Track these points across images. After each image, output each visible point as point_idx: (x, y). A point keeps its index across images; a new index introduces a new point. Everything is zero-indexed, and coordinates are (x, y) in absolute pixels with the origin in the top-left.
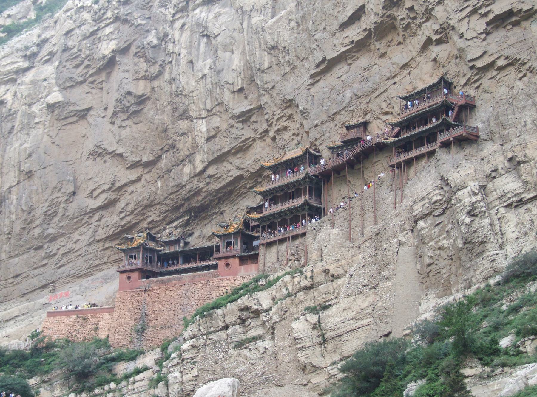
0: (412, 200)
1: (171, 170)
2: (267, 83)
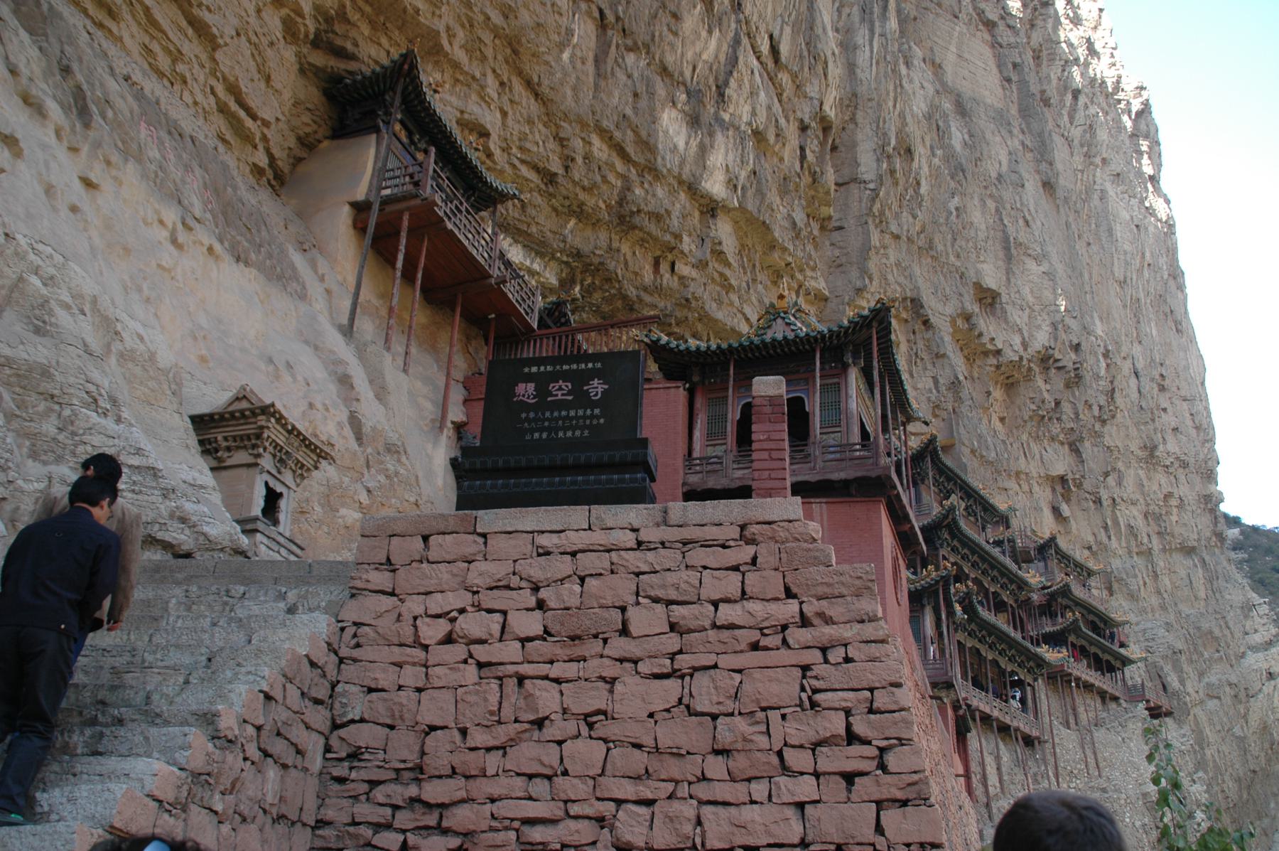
2: (890, 208)
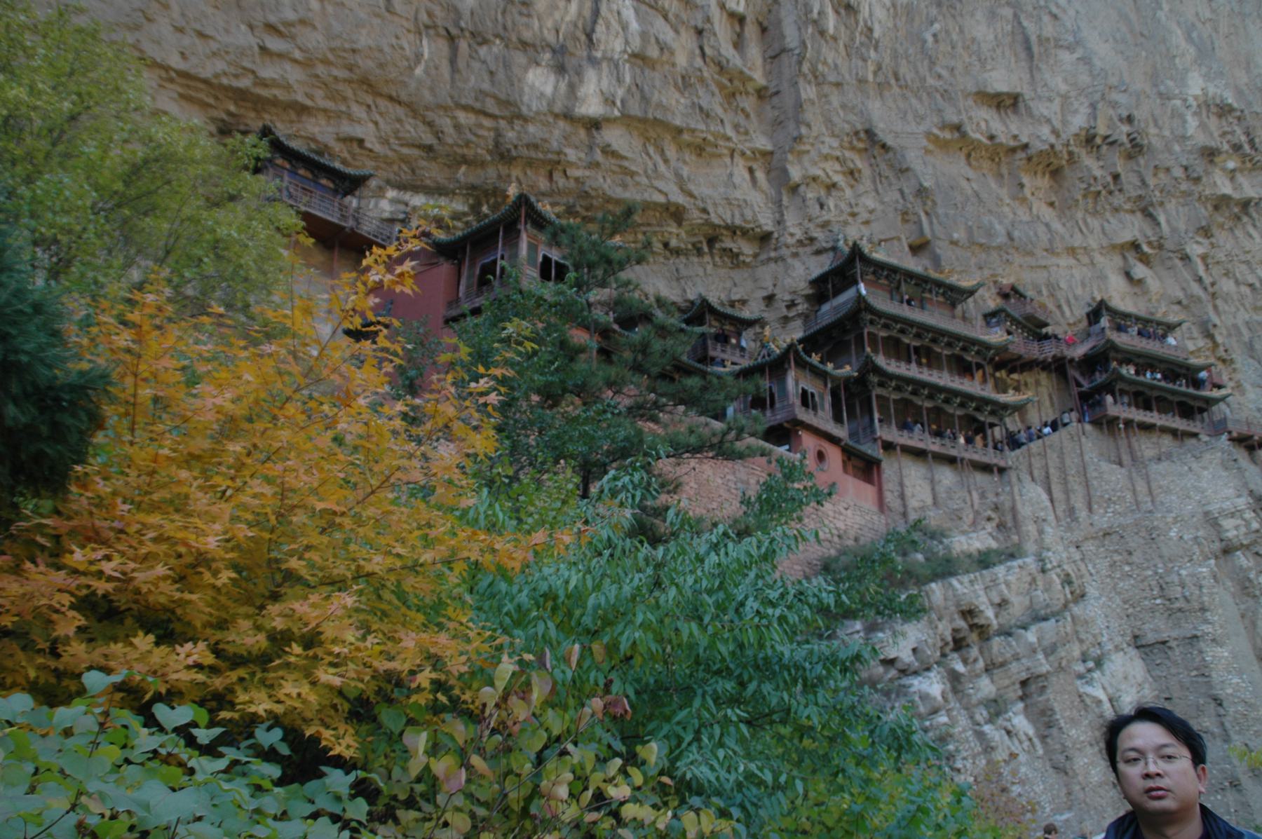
1: (485, 42)
2: (825, 63)
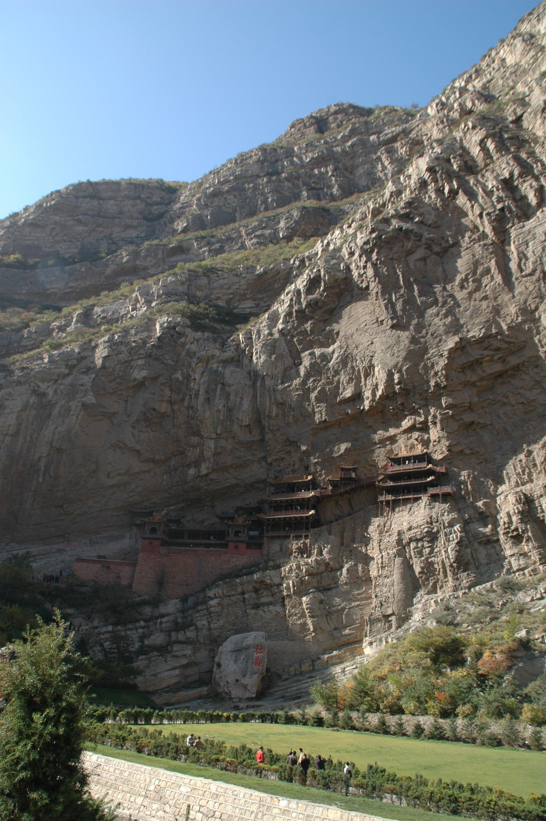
0: (405, 526)
